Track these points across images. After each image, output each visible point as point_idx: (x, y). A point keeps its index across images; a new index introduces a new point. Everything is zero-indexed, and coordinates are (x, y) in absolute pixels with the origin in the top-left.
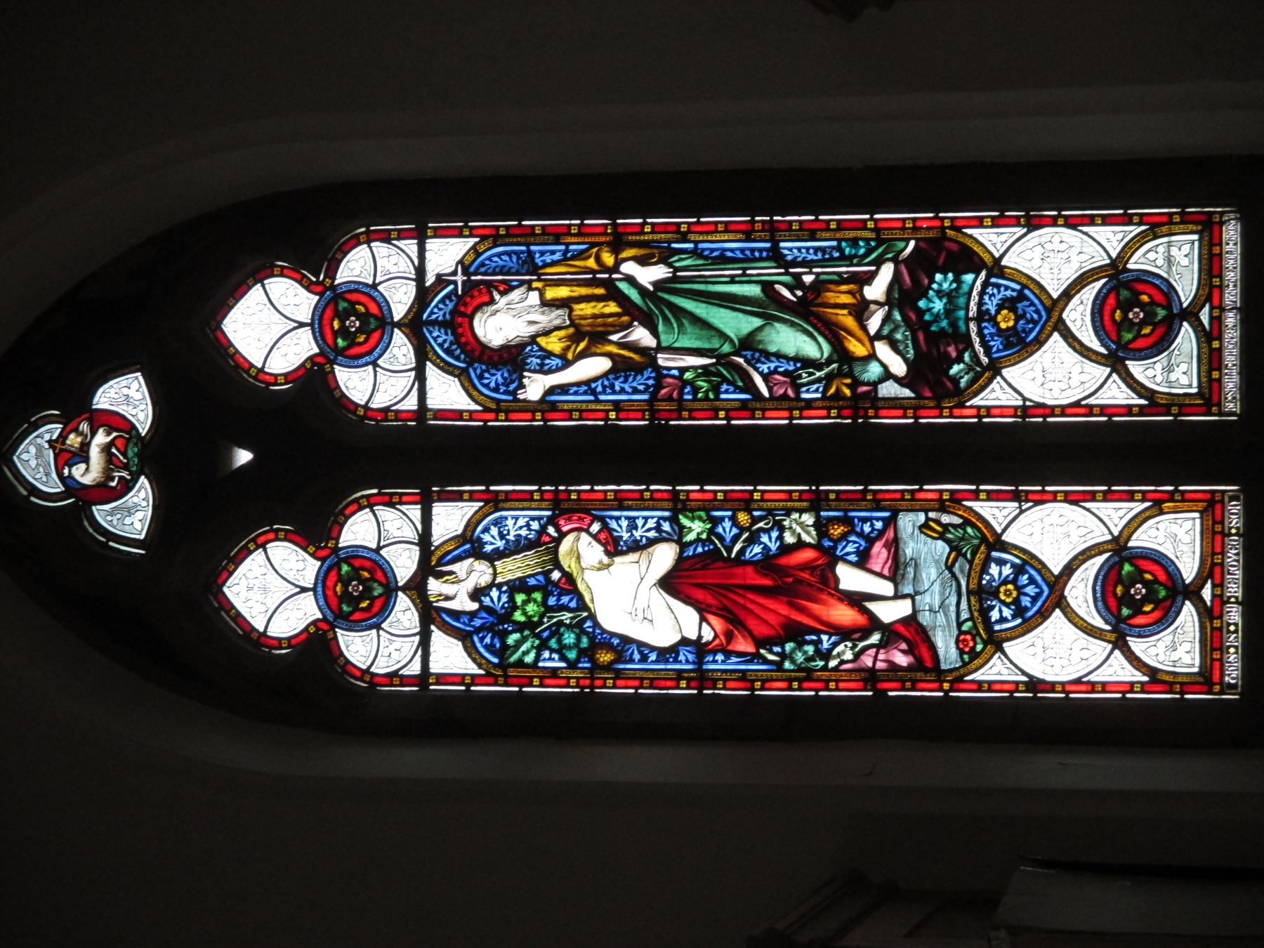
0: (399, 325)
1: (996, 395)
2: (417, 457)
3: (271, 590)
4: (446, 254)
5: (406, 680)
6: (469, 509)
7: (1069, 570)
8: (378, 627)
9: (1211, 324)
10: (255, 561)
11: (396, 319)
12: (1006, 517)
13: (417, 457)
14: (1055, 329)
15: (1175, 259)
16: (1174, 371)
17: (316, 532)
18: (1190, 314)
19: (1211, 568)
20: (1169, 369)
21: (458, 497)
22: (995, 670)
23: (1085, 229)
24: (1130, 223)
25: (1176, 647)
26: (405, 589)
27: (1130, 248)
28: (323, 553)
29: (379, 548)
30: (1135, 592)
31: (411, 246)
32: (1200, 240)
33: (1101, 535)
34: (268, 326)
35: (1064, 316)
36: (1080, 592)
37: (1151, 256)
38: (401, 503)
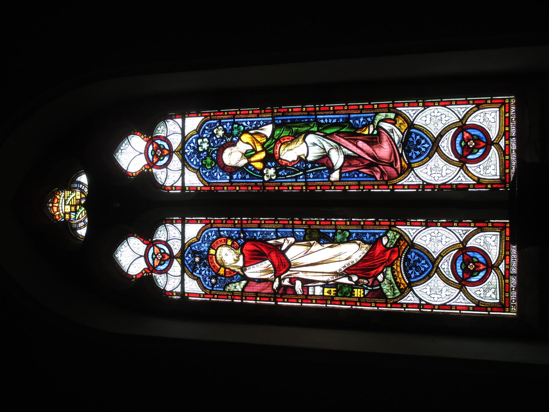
1: (411, 179)
3: (131, 256)
5: (177, 294)
6: (199, 226)
8: (167, 273)
9: (505, 147)
14: (436, 151)
15: (489, 119)
16: (489, 168)
20: (485, 168)
21: (196, 222)
22: (409, 299)
23: (449, 107)
24: (469, 104)
25: (488, 291)
27: (468, 115)
28: (148, 242)
29: (167, 241)
30: (469, 266)
31: (179, 121)
32: (500, 111)
33: (455, 241)
34: (132, 155)
38: (176, 223)
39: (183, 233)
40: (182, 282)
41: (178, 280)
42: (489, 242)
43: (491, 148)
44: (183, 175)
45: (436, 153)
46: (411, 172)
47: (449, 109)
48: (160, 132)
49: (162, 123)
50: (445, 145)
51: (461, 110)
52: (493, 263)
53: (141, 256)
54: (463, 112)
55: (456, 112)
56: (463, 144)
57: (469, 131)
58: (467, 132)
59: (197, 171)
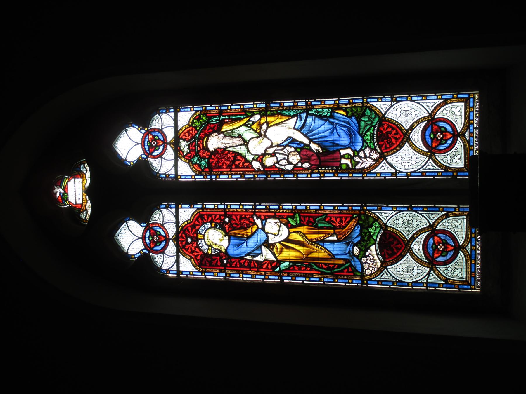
0: (170, 144)
2: (177, 192)
3: (130, 237)
4: (185, 117)
7: (413, 238)
8: (163, 253)
10: (124, 227)
11: (168, 141)
12: (387, 217)
13: (177, 192)
14: (407, 141)
15: (455, 113)
17: (144, 217)
18: (462, 135)
19: (469, 238)
25: (457, 271)
26: (172, 239)
32: (465, 105)
33: (426, 225)
34: (129, 145)
35: (410, 136)
36: (417, 247)
37: (445, 112)
39: (177, 217)
40: (178, 261)
41: (174, 259)
42: (457, 226)
43: (457, 139)
44: (176, 165)
45: (408, 254)
46: (383, 160)
47: (421, 214)
48: (156, 219)
49: (158, 211)
50: (416, 137)
51: (430, 103)
52: (460, 244)
53: (139, 238)
54: (432, 106)
55: (426, 107)
56: (432, 136)
57: (440, 235)
58: (438, 236)
59: (190, 161)
